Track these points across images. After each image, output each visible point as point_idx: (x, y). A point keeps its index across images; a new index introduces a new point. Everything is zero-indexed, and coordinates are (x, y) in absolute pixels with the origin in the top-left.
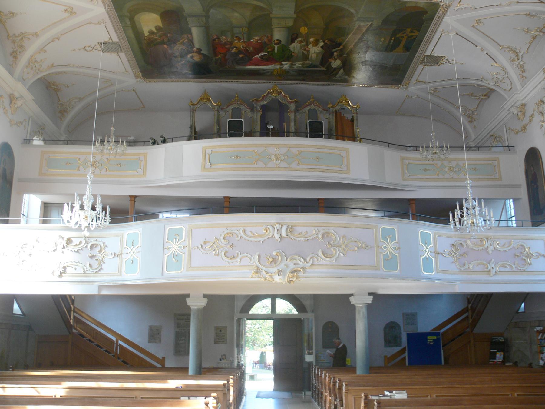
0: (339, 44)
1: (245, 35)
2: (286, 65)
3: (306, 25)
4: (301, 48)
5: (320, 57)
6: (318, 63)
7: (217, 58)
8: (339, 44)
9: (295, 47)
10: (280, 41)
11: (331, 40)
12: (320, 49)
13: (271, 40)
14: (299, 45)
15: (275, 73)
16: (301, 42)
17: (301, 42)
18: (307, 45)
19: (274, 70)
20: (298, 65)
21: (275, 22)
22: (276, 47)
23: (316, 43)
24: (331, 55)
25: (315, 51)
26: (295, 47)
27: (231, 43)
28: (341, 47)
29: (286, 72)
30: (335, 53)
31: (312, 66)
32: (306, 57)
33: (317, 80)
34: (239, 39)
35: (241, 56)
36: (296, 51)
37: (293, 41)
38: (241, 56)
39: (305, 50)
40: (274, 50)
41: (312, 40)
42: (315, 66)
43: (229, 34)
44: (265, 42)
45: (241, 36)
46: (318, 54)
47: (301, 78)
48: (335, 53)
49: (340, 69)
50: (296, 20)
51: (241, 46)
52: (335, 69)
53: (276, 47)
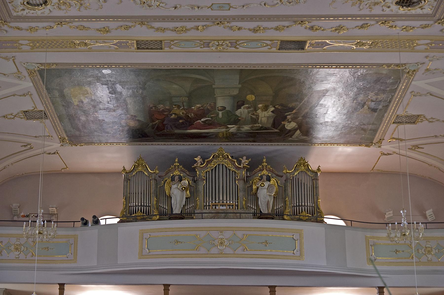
0: (292, 109)
1: (185, 104)
2: (233, 128)
3: (252, 93)
4: (249, 112)
5: (271, 121)
6: (269, 126)
7: (154, 123)
8: (292, 109)
9: (242, 112)
10: (224, 108)
11: (281, 105)
12: (270, 113)
13: (214, 106)
14: (246, 111)
15: (221, 135)
16: (248, 108)
17: (248, 108)
18: (256, 109)
19: (219, 133)
20: (246, 128)
21: (217, 92)
22: (220, 113)
23: (266, 108)
24: (285, 118)
25: (265, 116)
26: (242, 112)
27: (170, 110)
28: (294, 111)
29: (233, 134)
30: (288, 117)
31: (261, 128)
32: (255, 121)
33: (271, 141)
34: (179, 107)
35: (181, 121)
36: (244, 116)
37: (239, 107)
38: (181, 121)
39: (253, 114)
40: (218, 115)
41: (260, 106)
42: (266, 129)
43: (168, 103)
44: (208, 109)
45: (181, 104)
46: (268, 118)
47: (251, 139)
48: (288, 117)
49: (295, 130)
50: (240, 90)
51: (181, 113)
52: (290, 131)
53: (220, 113)
